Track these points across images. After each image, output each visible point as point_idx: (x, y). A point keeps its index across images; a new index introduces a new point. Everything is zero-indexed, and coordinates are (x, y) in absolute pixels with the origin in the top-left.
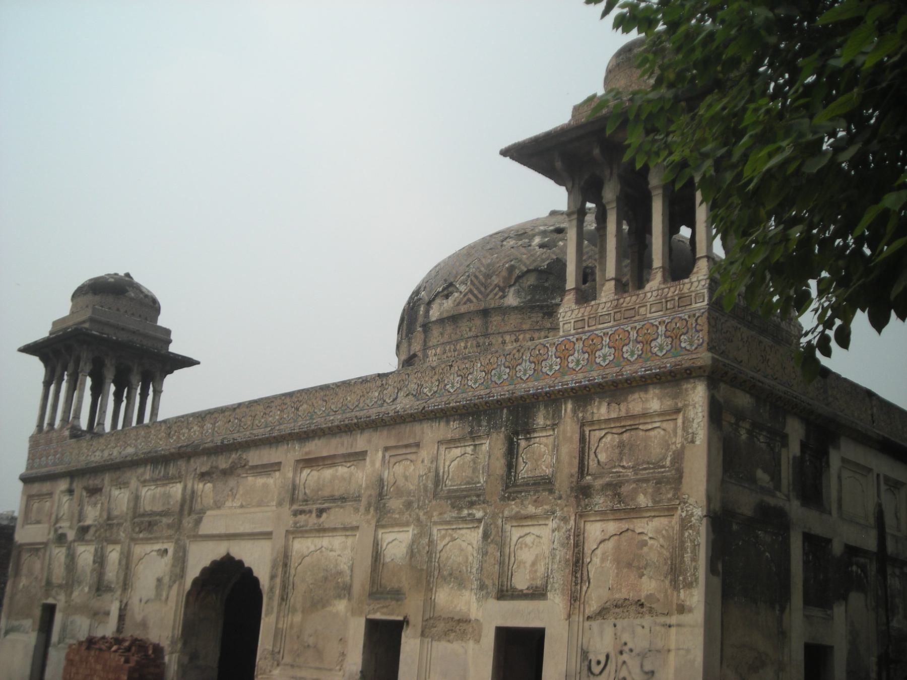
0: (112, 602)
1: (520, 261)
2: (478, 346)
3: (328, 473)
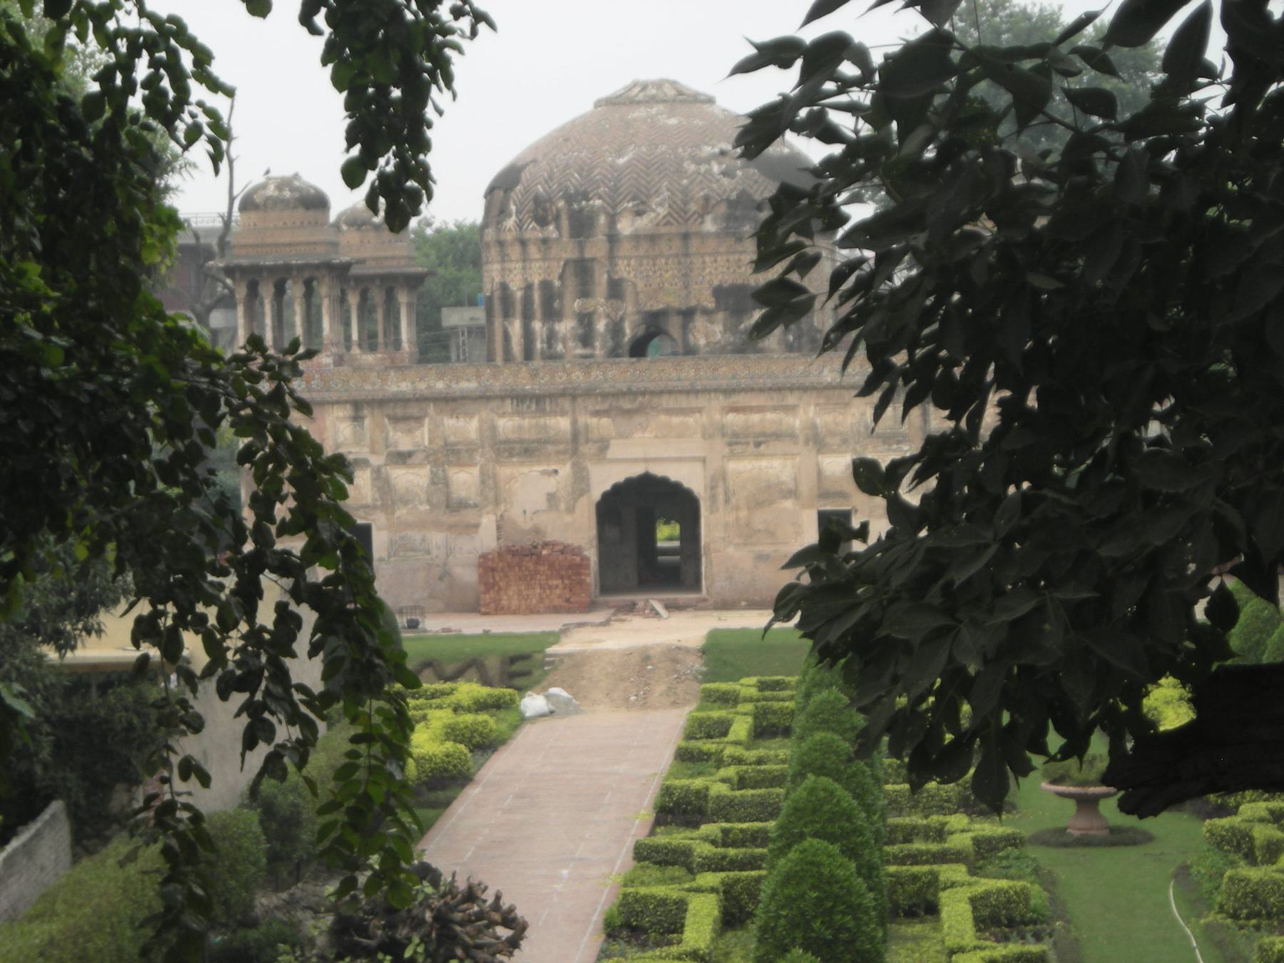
0: (480, 516)
1: (713, 190)
2: (679, 263)
3: (755, 418)
